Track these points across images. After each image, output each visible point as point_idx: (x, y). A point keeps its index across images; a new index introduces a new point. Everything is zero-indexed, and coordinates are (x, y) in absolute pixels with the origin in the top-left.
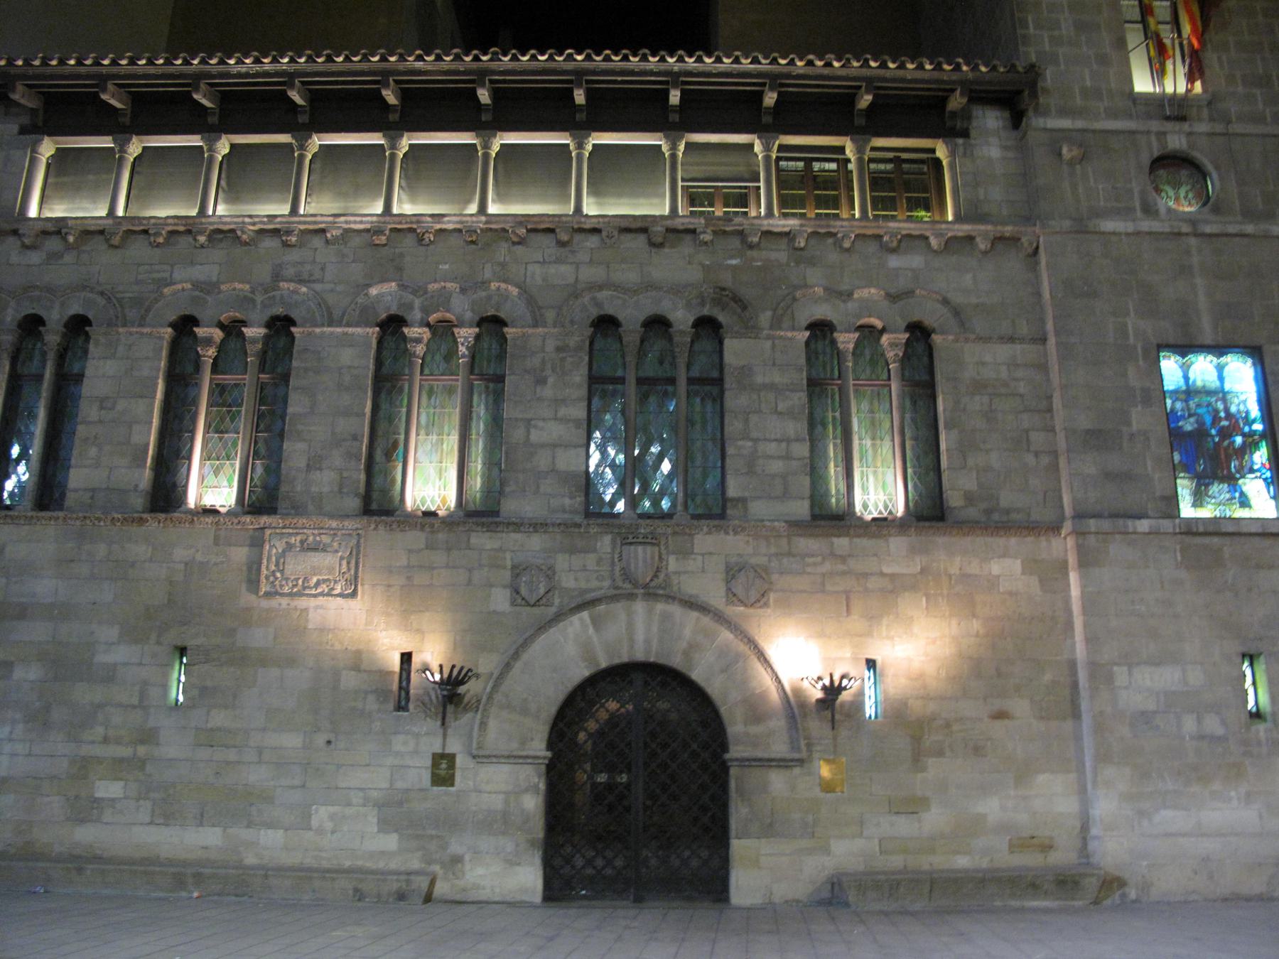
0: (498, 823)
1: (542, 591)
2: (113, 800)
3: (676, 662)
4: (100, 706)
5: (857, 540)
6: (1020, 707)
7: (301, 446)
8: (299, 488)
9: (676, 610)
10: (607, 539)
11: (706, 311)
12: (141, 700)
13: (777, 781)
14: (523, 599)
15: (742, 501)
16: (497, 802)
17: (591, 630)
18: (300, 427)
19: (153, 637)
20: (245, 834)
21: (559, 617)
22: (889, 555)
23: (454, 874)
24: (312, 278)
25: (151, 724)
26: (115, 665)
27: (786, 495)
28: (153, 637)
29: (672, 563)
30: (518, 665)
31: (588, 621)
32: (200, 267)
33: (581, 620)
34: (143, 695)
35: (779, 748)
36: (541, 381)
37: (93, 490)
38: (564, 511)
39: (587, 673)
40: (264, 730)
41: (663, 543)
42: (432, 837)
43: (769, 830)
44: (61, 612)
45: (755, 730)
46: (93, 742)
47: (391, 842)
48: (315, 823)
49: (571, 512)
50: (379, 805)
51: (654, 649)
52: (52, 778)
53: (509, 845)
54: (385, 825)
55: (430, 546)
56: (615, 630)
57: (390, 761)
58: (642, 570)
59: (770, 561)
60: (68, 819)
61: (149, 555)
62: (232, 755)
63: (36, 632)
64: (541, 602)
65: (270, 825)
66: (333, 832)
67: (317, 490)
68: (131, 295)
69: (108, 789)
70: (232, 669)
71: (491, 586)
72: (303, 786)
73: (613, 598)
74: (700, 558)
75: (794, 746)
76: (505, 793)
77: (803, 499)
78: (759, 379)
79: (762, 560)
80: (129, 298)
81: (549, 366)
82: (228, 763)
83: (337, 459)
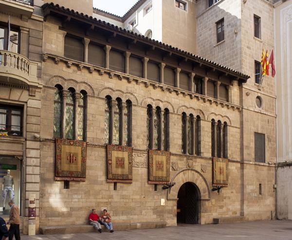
0: (170, 212)
3: (194, 182)
4: (100, 190)
6: (234, 191)
7: (135, 133)
9: (194, 172)
13: (207, 203)
15: (203, 153)
16: (170, 208)
20: (131, 217)
21: (179, 173)
25: (111, 194)
27: (208, 153)
35: (207, 198)
37: (93, 138)
43: (206, 212)
45: (204, 194)
47: (155, 216)
50: (153, 210)
54: (154, 213)
56: (186, 176)
57: (154, 201)
58: (190, 165)
62: (127, 201)
65: (135, 215)
73: (187, 170)
75: (209, 197)
78: (205, 130)
83: (142, 136)
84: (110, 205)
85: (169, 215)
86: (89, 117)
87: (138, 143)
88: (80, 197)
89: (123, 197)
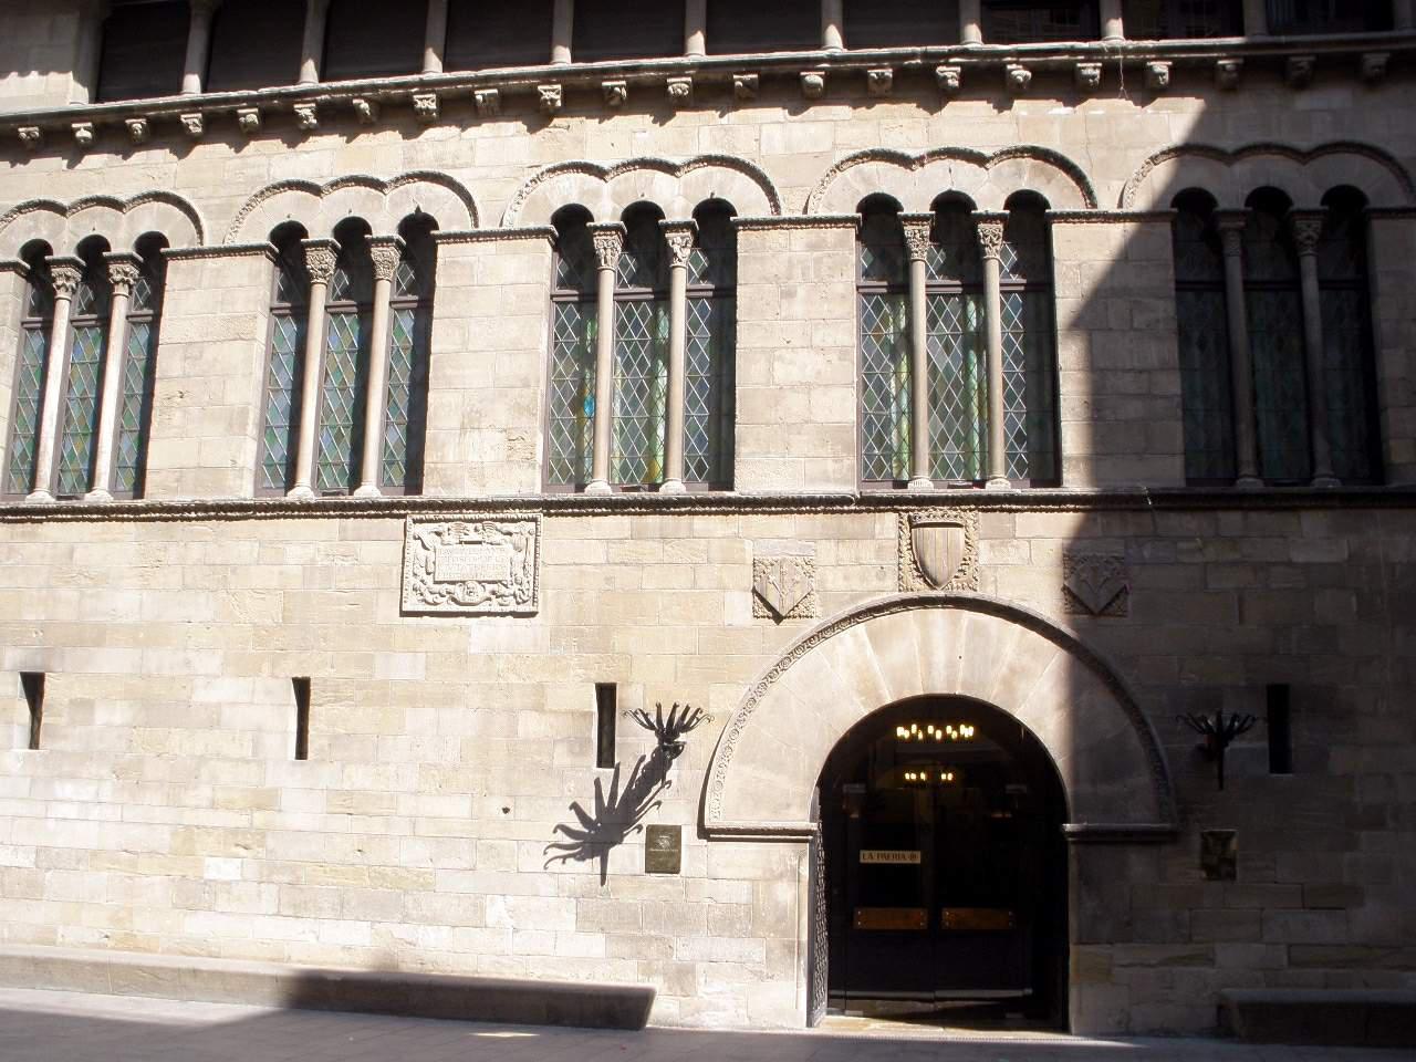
1: (798, 595)
2: (229, 883)
3: (992, 695)
4: (202, 759)
5: (1254, 516)
8: (451, 458)
10: (890, 519)
11: (1024, 185)
12: (255, 753)
14: (770, 608)
16: (741, 893)
17: (869, 650)
18: (449, 372)
19: (266, 668)
21: (823, 633)
22: (1302, 537)
23: (682, 989)
24: (457, 162)
26: (219, 705)
28: (266, 668)
29: (984, 553)
30: (765, 703)
31: (866, 639)
32: (306, 156)
33: (855, 636)
34: (257, 746)
36: (789, 294)
38: (828, 480)
39: (865, 712)
40: (417, 793)
41: (970, 523)
42: (651, 939)
44: (148, 635)
46: (197, 807)
47: (596, 944)
48: (490, 920)
49: (837, 481)
51: (961, 675)
52: (152, 853)
53: (755, 950)
55: (637, 536)
58: (935, 564)
59: (1126, 547)
60: (175, 906)
61: (256, 555)
62: (377, 826)
63: (114, 661)
64: (797, 611)
65: (433, 920)
66: (516, 930)
67: (476, 459)
68: (217, 201)
69: (221, 868)
70: (370, 710)
71: (724, 589)
72: (473, 869)
74: (1022, 541)
76: (752, 880)
77: (1174, 454)
79: (1118, 549)
80: (217, 205)
81: (798, 272)
82: (371, 837)
83: (502, 415)
84: (262, 852)
85: (727, 947)
86: (166, 362)
87: (473, 457)
88: (88, 792)
89: (348, 803)
